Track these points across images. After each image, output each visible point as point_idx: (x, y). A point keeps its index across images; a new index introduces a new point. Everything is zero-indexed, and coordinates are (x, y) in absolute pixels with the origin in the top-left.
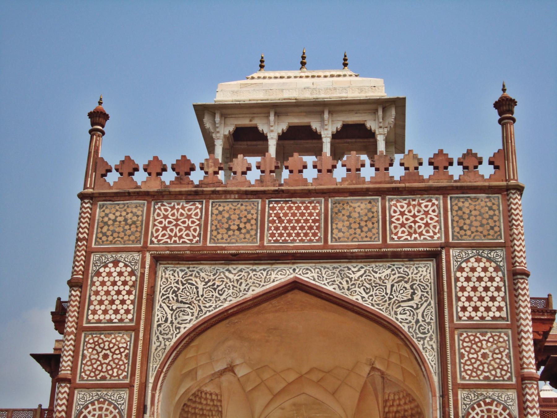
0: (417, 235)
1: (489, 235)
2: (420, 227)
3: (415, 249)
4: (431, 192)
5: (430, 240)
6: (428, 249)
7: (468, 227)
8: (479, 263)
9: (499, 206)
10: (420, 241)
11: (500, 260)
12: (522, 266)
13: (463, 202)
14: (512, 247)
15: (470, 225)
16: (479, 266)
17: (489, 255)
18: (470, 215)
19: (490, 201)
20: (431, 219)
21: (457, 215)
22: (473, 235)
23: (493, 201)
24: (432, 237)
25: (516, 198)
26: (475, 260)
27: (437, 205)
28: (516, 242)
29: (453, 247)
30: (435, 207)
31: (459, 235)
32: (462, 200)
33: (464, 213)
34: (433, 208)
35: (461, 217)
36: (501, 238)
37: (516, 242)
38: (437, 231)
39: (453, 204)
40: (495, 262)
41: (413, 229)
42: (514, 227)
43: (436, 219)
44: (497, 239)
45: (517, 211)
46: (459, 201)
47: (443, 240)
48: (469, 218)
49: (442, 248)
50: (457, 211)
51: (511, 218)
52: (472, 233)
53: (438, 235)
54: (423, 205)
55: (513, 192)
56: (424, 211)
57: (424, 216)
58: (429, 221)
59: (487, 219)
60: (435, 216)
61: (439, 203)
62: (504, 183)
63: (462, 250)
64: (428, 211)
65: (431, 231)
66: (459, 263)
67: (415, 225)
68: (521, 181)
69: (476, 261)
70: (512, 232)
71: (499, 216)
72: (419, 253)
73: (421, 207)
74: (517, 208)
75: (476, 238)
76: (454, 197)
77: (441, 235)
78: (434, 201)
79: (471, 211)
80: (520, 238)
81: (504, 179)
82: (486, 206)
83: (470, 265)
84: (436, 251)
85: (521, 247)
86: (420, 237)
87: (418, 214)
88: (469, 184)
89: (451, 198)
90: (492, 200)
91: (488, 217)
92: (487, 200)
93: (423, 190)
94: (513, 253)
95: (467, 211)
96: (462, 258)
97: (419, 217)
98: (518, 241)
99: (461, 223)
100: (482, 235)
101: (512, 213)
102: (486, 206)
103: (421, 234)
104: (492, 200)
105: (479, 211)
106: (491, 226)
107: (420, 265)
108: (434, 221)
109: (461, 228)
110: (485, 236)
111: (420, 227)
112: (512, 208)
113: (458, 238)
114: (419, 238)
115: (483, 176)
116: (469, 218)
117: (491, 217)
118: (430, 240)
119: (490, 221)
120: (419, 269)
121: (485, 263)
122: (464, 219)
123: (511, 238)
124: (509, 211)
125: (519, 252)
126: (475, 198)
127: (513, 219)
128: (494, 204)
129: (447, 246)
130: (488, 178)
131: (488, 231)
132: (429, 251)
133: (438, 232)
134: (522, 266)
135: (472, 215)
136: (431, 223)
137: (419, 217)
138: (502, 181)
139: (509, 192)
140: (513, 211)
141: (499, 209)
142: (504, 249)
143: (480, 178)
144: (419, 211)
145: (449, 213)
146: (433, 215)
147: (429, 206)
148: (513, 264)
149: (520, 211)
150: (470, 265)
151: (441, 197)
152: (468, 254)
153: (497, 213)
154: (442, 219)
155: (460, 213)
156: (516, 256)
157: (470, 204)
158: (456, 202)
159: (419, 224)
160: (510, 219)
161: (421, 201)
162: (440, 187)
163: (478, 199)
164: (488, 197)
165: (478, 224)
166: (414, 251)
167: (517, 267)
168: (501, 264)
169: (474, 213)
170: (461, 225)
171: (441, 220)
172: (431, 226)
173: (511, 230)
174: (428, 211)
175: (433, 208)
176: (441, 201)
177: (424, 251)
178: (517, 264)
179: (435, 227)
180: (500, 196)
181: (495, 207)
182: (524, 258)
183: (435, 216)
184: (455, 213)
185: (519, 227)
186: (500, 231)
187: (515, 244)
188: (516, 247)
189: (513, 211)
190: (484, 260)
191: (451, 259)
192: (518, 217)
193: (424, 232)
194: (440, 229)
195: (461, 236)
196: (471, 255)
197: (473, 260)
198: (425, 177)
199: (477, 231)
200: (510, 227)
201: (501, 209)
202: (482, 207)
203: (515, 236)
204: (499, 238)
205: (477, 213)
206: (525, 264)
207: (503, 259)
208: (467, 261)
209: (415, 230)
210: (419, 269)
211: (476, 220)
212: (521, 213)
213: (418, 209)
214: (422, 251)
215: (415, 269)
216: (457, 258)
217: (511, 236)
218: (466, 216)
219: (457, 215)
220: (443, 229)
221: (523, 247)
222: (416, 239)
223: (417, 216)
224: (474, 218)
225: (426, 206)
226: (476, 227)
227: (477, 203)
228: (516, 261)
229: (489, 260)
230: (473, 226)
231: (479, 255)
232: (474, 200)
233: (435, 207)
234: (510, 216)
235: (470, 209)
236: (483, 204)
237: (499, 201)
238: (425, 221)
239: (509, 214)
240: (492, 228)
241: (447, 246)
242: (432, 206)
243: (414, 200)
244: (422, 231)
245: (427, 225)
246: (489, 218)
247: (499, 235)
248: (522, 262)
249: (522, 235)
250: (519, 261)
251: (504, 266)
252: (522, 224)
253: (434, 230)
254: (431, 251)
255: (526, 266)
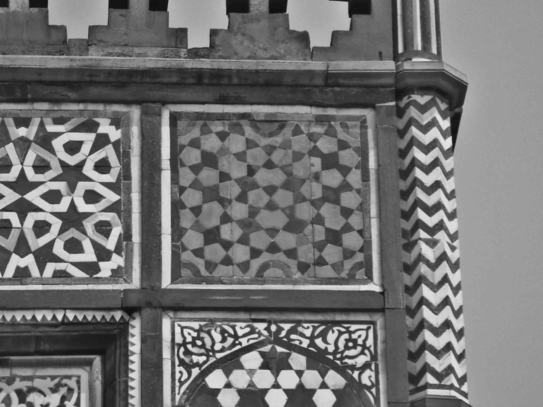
0: (29, 261)
1: (321, 262)
2: (41, 228)
3: (19, 316)
4: (94, 91)
5: (81, 281)
6: (71, 315)
7: (238, 233)
8: (276, 375)
9: (363, 152)
10: (42, 281)
11: (361, 360)
12: (451, 387)
13: (222, 136)
14: (412, 312)
15: (248, 225)
16: (276, 386)
17: (319, 342)
18: (247, 185)
19: (331, 133)
20: (92, 197)
21: (196, 185)
22: (255, 264)
23: (342, 135)
24: (91, 269)
25: (433, 123)
26: (260, 360)
27: (116, 145)
28: (426, 292)
29: (176, 309)
30: (108, 152)
31: (200, 263)
32: (218, 127)
33: (224, 177)
34: (99, 155)
35: (212, 194)
36: (370, 277)
37: (426, 292)
38: (111, 244)
39: (183, 140)
40: (342, 370)
41: (14, 235)
42: (423, 234)
43: (112, 197)
44: (351, 279)
45: (437, 174)
46: (206, 131)
47: (136, 282)
48: (242, 198)
49: (130, 311)
50: (195, 169)
51: (411, 200)
52: (255, 253)
53: (117, 261)
54: (58, 144)
55: (423, 100)
56: (63, 165)
57: (61, 186)
58: (82, 207)
59: (316, 204)
60: (106, 185)
61: (127, 136)
62: (389, 65)
63: (212, 321)
64: (82, 164)
65: (87, 245)
66: (196, 372)
67: (22, 219)
68: (454, 64)
69: (264, 366)
70: (414, 254)
71: (363, 193)
72: (36, 332)
73: (52, 151)
74: (436, 163)
75: (268, 273)
76: (188, 115)
77: (129, 260)
78: (105, 127)
79: (251, 171)
80: (445, 279)
81: (389, 51)
82: (315, 152)
83: (240, 379)
84: (104, 323)
85: (447, 313)
86: (42, 270)
87: (39, 178)
88: (249, 65)
89: (174, 118)
90: (339, 129)
91: (317, 192)
92: (318, 129)
93: (64, 84)
94: (414, 335)
95: (238, 171)
96: (209, 352)
97: (42, 190)
98: (435, 288)
99: (212, 214)
100: (293, 264)
101: (416, 182)
102: (315, 152)
103: (45, 256)
104: (339, 129)
105: (287, 170)
106: (328, 231)
107: (37, 383)
108: (103, 204)
109: (211, 236)
110: (303, 268)
111: (41, 228)
112: (414, 162)
113: (197, 272)
114: (35, 272)
115: (304, 37)
116: (242, 198)
117: (332, 195)
118: (81, 281)
119: (327, 210)
120: (33, 398)
121: (300, 373)
122: (223, 202)
123: (409, 280)
124: (405, 174)
125: (437, 332)
126: (270, 120)
127: (418, 203)
128: (343, 145)
129: (151, 303)
130: (327, 43)
131: (320, 246)
132: (75, 323)
133: (118, 250)
134: (451, 387)
135: (255, 186)
136: (87, 215)
137: (42, 190)
138: (381, 56)
139: (405, 100)
140: (418, 173)
141: (363, 166)
142: (379, 320)
143: (294, 46)
144: (41, 167)
145: (166, 177)
146: (97, 181)
147: (86, 148)
148: (415, 379)
149: (448, 175)
150: (240, 379)
151: (135, 112)
152: (236, 336)
153: (354, 178)
154: (135, 197)
155: (209, 176)
156: (425, 346)
157: (250, 144)
158: (196, 133)
159: (40, 216)
160: (406, 206)
161: (51, 128)
162: (132, 73)
163: (282, 125)
164: (319, 120)
165: (278, 220)
166: (14, 323)
167: (431, 392)
168: (367, 378)
169: (263, 177)
170: (215, 222)
171: (129, 201)
172: (89, 225)
173: (409, 246)
174: (82, 164)
175: (99, 155)
176: (135, 130)
177: (55, 324)
178: (430, 379)
179: (104, 228)
180: (368, 114)
181: (348, 157)
182: (460, 358)
183: (106, 185)
184: (186, 177)
185: (441, 236)
186: (366, 248)
187: (423, 301)
188: (426, 313)
189: (418, 173)
190: (298, 361)
191: (166, 354)
192: (439, 195)
193: (58, 249)
194: (127, 235)
195: (210, 266)
196: (244, 342)
197: (253, 360)
198: (71, 35)
199: (273, 248)
200: (406, 234)
201: (372, 164)
202: (298, 156)
203: (423, 269)
204: (360, 274)
205: (277, 177)
206: (462, 380)
207: (374, 357)
208: (231, 363)
209: (22, 239)
210: (33, 398)
211: (271, 207)
212: (449, 185)
213: (39, 158)
214: (44, 324)
215: (14, 398)
216: (187, 353)
217: (409, 269)
218: (232, 190)
219: (196, 185)
220: (136, 238)
221: (457, 314)
222: (22, 274)
223: (36, 185)
224: (266, 199)
225: (73, 148)
226: (272, 232)
227: (278, 140)
228: (426, 368)
229: (318, 360)
230: (259, 228)
231: (278, 341)
232: (267, 128)
233: (108, 152)
234: (405, 195)
235: (250, 161)
236: (300, 143)
237: (364, 136)
238: (63, 206)
239: (404, 185)
240: (334, 237)
241: (151, 303)
242: (95, 149)
243: (23, 122)
244: (51, 244)
245: (72, 219)
246: (324, 199)
247: (359, 265)
248: (450, 369)
249: (455, 267)
250: (438, 365)
251: (376, 384)
252: (452, 226)
253: (100, 239)
254: (85, 323)
255: (465, 388)
